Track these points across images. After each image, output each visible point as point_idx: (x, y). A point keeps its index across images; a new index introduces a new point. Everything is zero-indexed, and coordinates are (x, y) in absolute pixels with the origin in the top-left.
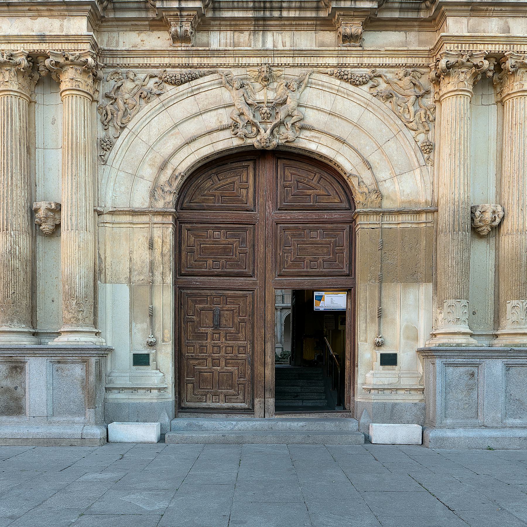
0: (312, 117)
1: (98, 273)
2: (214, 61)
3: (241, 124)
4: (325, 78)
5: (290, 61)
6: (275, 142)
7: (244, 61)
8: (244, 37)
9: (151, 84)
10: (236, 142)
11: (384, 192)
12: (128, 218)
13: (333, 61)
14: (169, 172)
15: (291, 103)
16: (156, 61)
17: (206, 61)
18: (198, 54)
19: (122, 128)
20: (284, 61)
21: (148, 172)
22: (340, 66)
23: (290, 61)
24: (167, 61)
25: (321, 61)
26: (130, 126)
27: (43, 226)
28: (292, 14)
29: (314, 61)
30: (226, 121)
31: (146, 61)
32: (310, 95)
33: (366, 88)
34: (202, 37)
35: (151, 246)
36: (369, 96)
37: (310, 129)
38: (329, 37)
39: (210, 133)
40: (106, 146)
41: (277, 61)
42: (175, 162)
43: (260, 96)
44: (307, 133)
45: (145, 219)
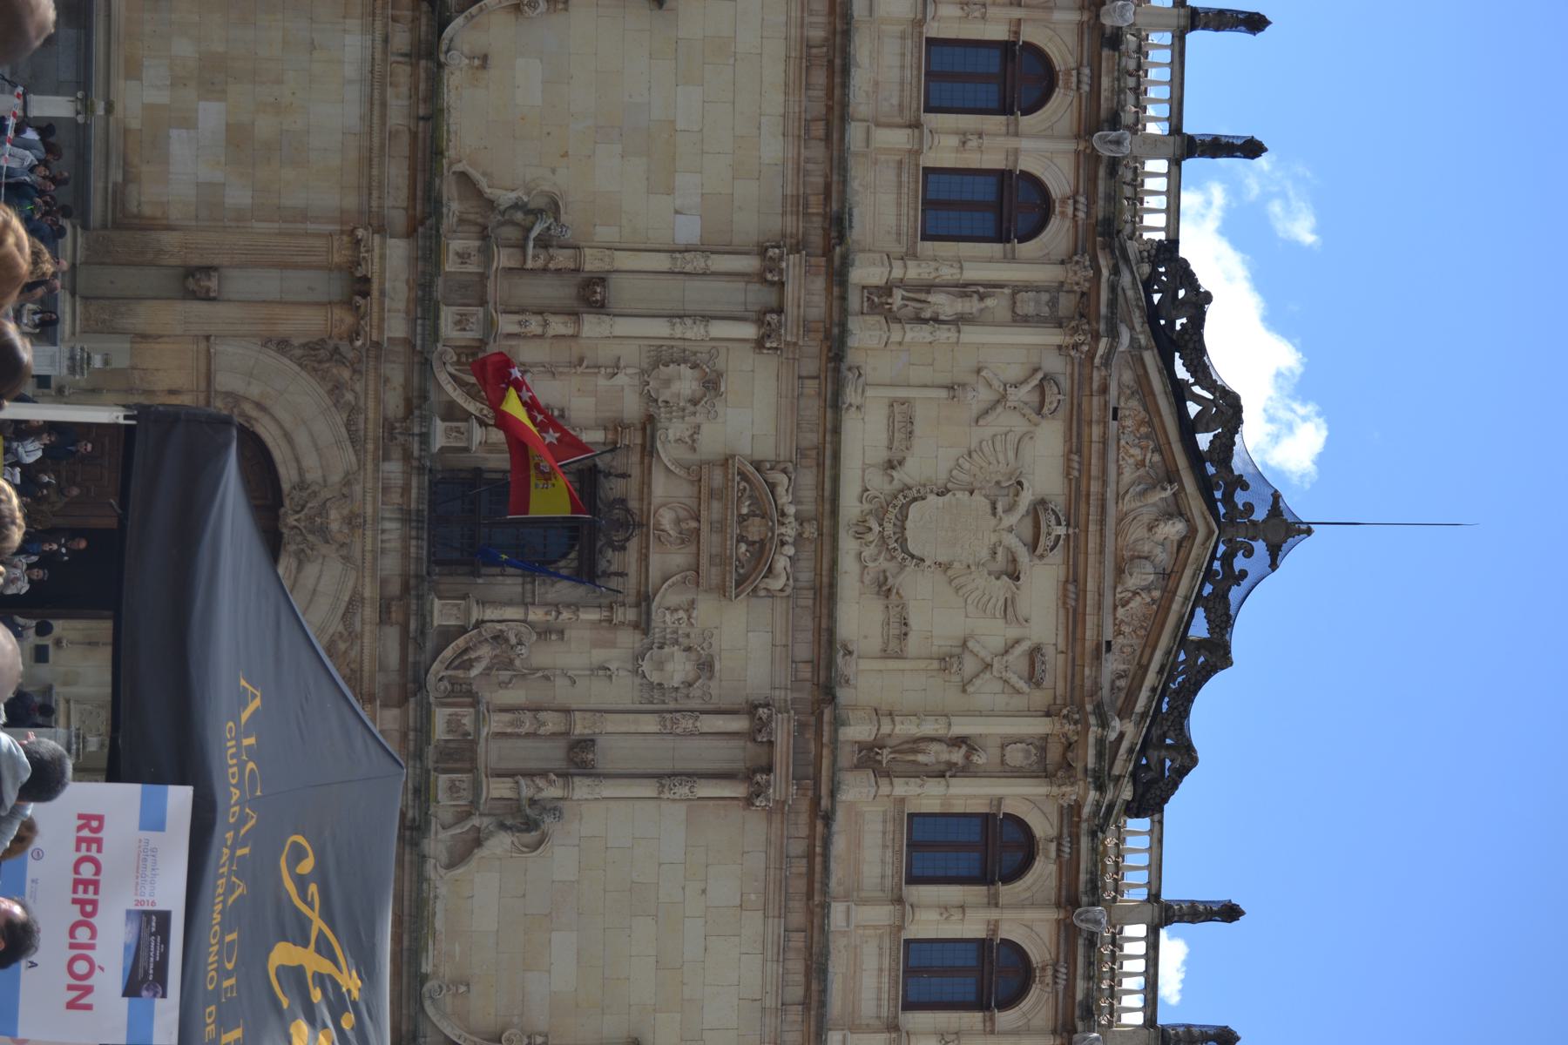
0: (311, 570)
1: (144, 337)
2: (370, 467)
3: (305, 494)
4: (351, 584)
5: (368, 547)
6: (285, 531)
7: (369, 498)
8: (396, 498)
9: (349, 396)
10: (286, 486)
12: (203, 369)
13: (367, 594)
14: (254, 413)
15: (324, 549)
16: (371, 404)
17: (370, 457)
18: (376, 449)
19: (300, 365)
20: (369, 541)
21: (255, 391)
22: (363, 599)
23: (368, 547)
24: (371, 415)
25: (368, 580)
26: (303, 374)
27: (194, 282)
28: (413, 550)
29: (367, 573)
30: (309, 477)
31: (371, 392)
32: (335, 567)
33: (341, 628)
34: (396, 453)
35: (172, 392)
36: (331, 631)
38: (395, 588)
39: (297, 460)
40: (283, 345)
41: (369, 533)
42: (265, 420)
43: (333, 514)
44: (294, 565)
45: (203, 385)
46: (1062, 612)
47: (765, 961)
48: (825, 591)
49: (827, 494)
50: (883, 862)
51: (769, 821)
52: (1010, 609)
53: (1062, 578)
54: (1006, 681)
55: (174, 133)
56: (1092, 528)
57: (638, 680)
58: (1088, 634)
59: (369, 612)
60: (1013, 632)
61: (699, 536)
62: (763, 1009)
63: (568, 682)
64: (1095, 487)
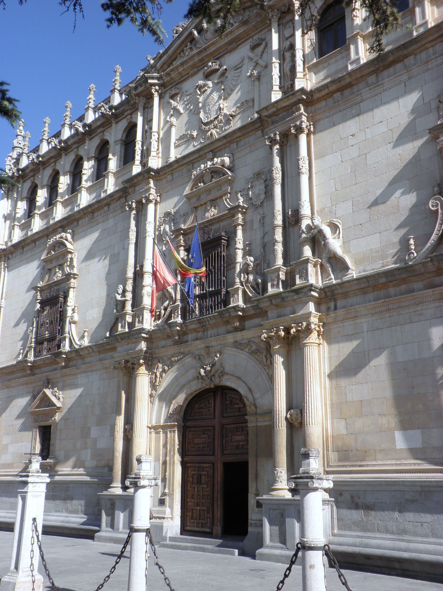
11: (258, 405)
37: (227, 374)
46: (239, 47)
47: (384, 90)
48: (228, 139)
49: (197, 155)
50: (336, 61)
51: (320, 120)
52: (238, 67)
53: (228, 54)
54: (263, 52)
55: (98, 447)
56: (208, 52)
57: (265, 204)
58: (242, 31)
59: (239, 336)
60: (246, 61)
61: (213, 200)
62: (409, 78)
63: (266, 236)
64: (196, 59)
